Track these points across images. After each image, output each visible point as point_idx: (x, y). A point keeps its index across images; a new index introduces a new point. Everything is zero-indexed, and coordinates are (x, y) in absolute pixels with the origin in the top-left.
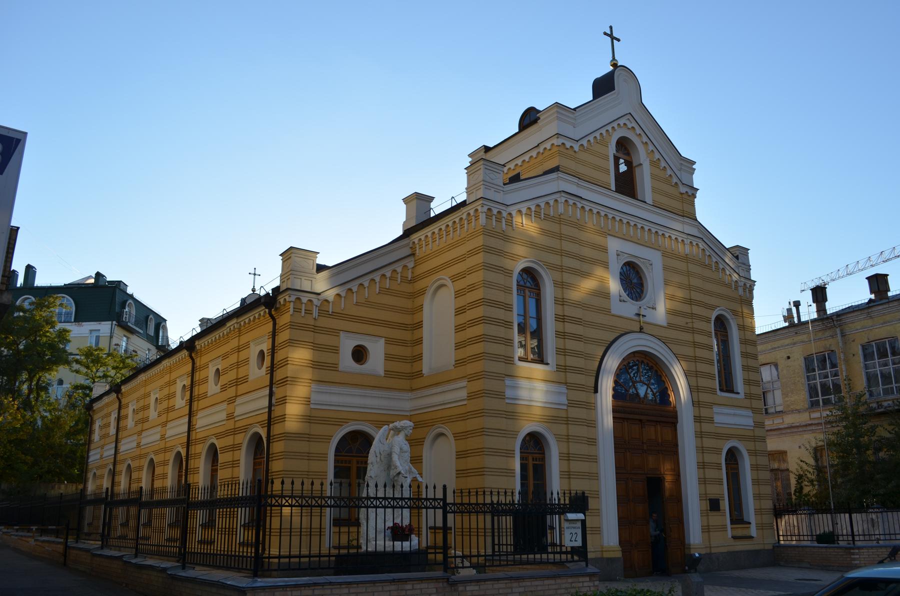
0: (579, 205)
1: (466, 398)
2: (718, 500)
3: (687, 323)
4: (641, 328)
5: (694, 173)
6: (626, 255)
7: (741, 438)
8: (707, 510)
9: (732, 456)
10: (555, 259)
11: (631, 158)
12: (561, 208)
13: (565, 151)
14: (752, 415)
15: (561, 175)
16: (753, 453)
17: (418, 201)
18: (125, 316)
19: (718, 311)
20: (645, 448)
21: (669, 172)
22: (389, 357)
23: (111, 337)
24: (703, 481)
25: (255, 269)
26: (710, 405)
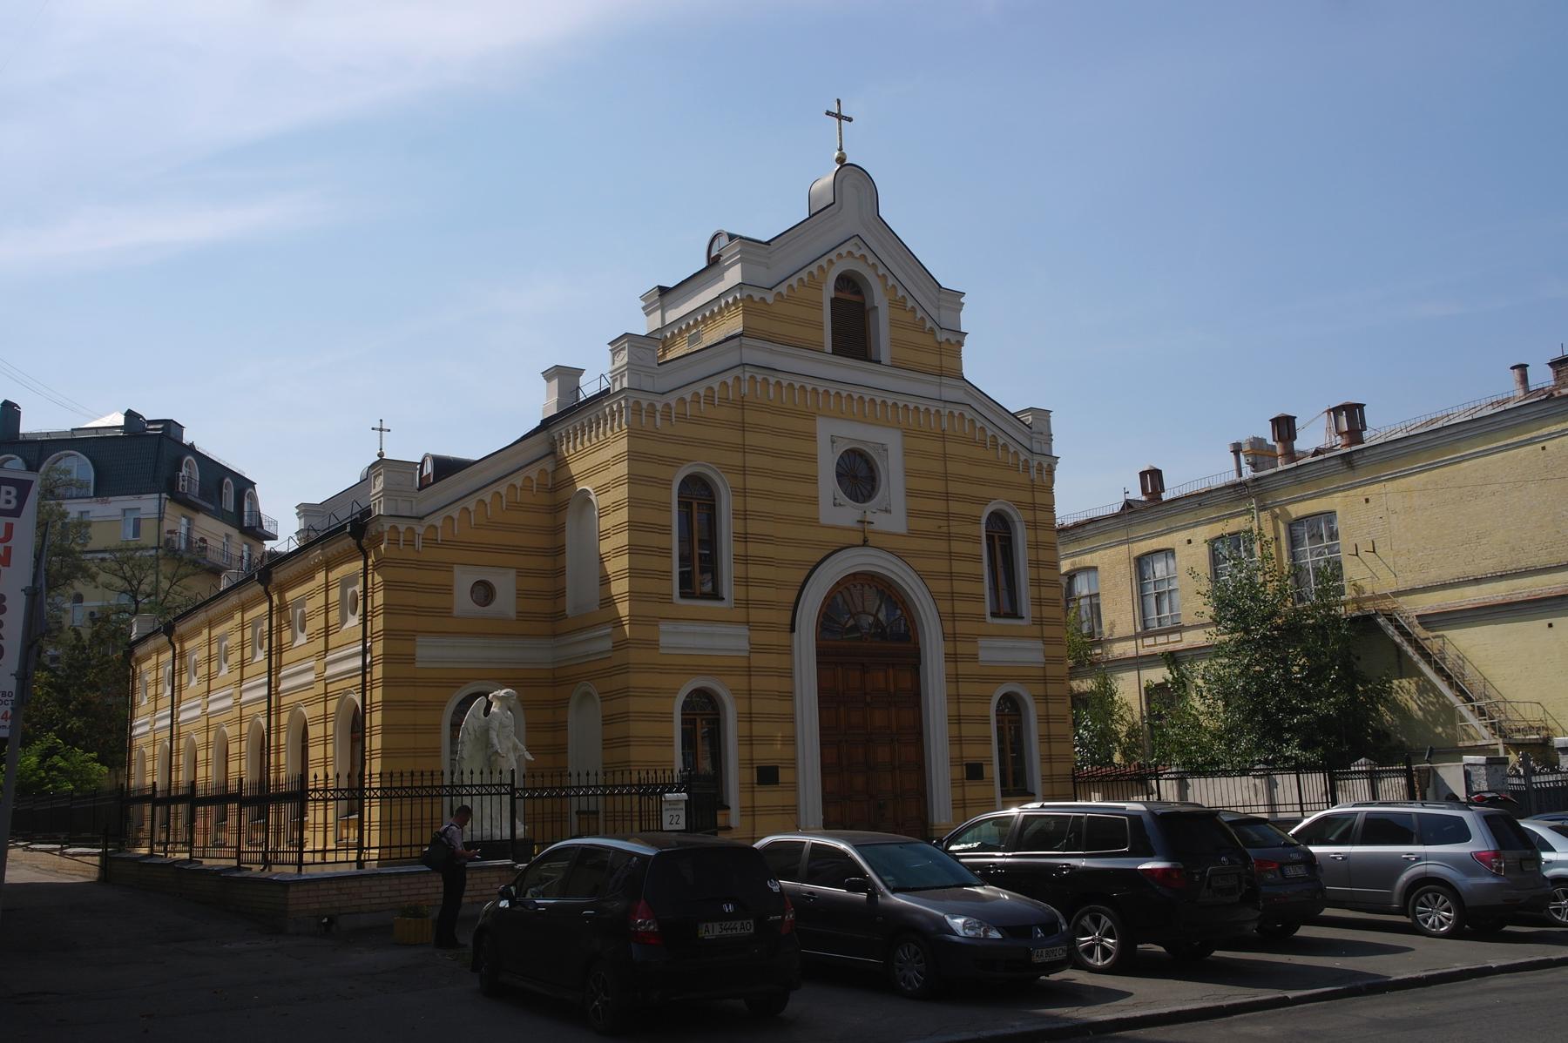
0: (772, 380)
1: (610, 648)
3: (940, 527)
5: (961, 310)
6: (847, 441)
7: (1022, 679)
8: (962, 779)
9: (1011, 707)
10: (736, 459)
11: (863, 296)
12: (745, 388)
16: (1045, 699)
17: (565, 376)
18: (181, 484)
19: (994, 504)
20: (868, 699)
21: (920, 314)
22: (522, 594)
23: (160, 519)
24: (958, 741)
25: (381, 421)
26: (972, 638)
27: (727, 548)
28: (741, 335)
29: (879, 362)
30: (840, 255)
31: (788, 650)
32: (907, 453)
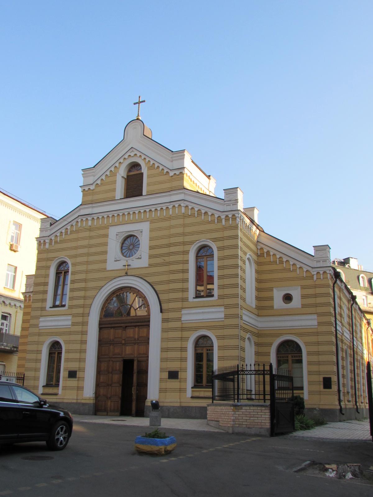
4: (126, 273)
12: (79, 224)
13: (87, 192)
15: (81, 207)
20: (123, 342)
21: (161, 167)
28: (81, 205)
30: (125, 158)
32: (151, 230)
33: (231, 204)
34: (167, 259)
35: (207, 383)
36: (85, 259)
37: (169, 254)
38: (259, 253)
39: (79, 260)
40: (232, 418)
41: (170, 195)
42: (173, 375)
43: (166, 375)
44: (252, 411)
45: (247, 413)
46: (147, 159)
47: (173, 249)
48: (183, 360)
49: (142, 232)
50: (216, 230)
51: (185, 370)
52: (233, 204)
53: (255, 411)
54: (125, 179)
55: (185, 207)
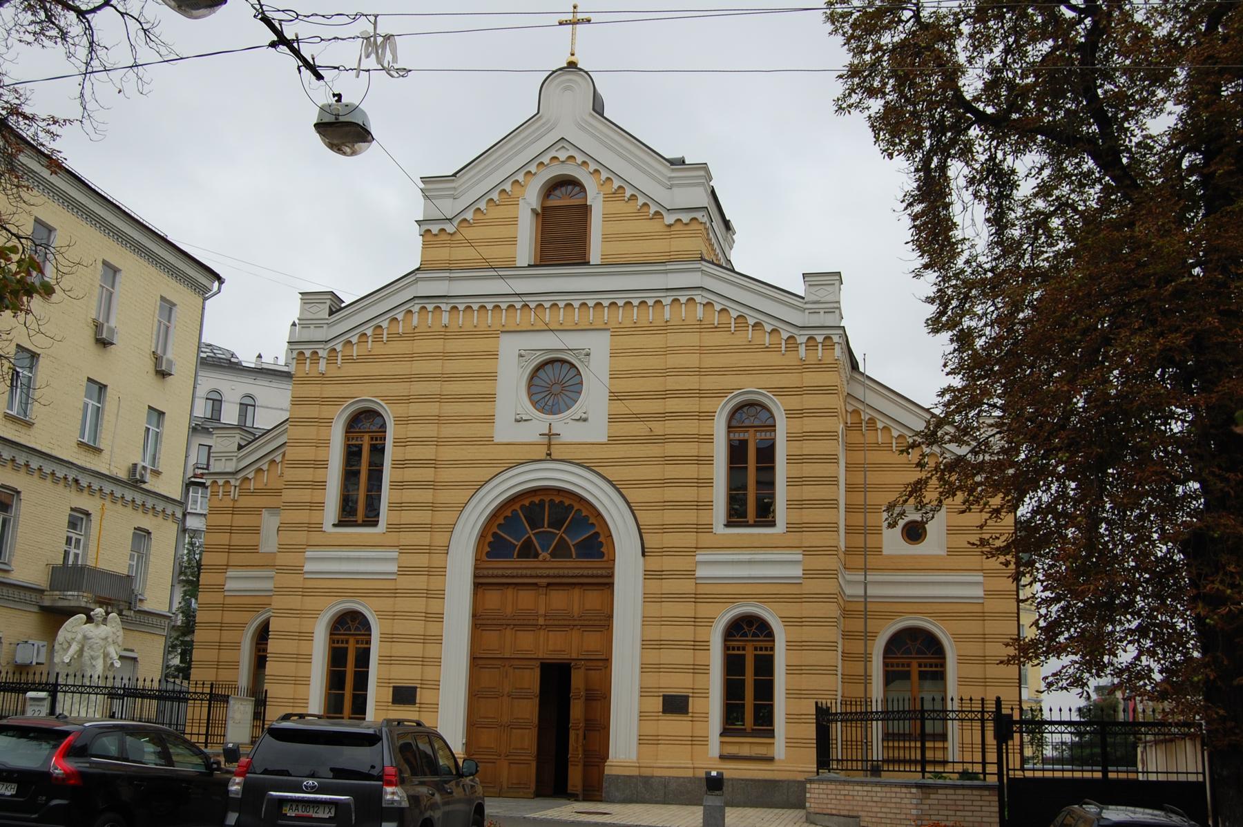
2: (687, 697)
4: (549, 455)
6: (539, 353)
14: (800, 557)
27: (719, 471)
28: (418, 269)
29: (587, 263)
30: (542, 163)
31: (442, 571)
32: (614, 354)
33: (822, 311)
34: (659, 428)
35: (754, 725)
36: (432, 409)
37: (664, 416)
38: (849, 422)
39: (415, 409)
40: (914, 812)
41: (666, 272)
42: (675, 705)
43: (658, 704)
44: (961, 797)
45: (949, 802)
46: (604, 175)
47: (673, 405)
48: (700, 669)
49: (588, 355)
50: (782, 370)
51: (705, 694)
52: (827, 310)
53: (966, 797)
54: (537, 214)
55: (704, 305)
